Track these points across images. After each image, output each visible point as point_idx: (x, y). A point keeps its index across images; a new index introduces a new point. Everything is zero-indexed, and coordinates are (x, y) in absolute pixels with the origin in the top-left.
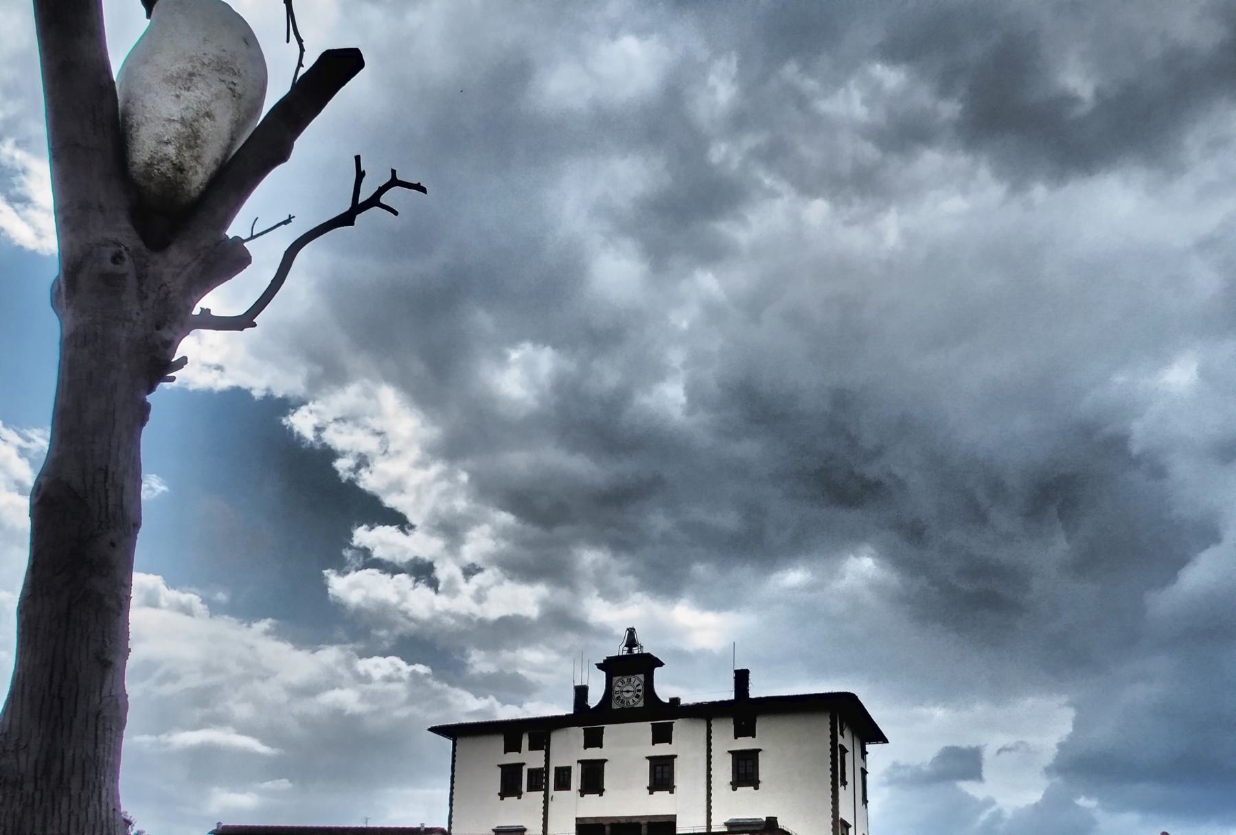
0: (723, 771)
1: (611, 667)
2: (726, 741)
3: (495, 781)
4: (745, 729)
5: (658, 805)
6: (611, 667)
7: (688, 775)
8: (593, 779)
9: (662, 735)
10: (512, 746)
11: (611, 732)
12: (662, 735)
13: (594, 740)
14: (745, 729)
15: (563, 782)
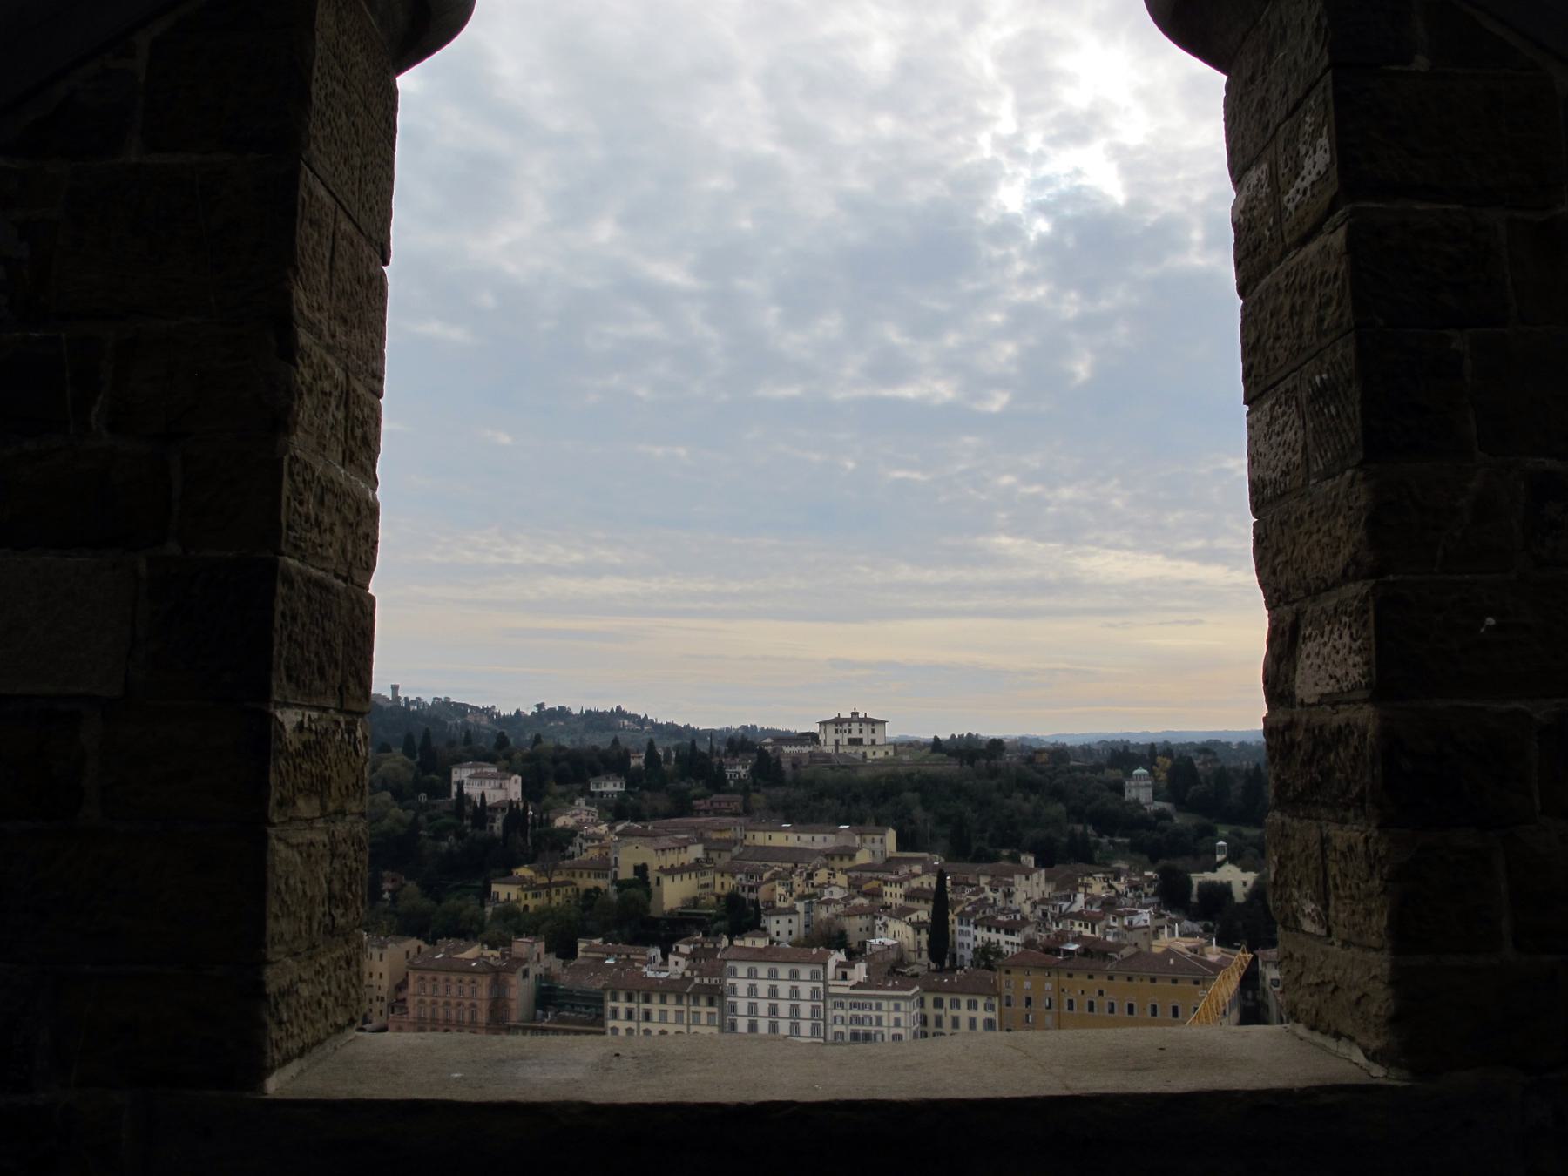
0: (870, 731)
1: (853, 714)
2: (870, 727)
3: (834, 731)
4: (873, 725)
5: (860, 736)
6: (853, 714)
7: (864, 731)
8: (850, 731)
9: (861, 725)
10: (837, 725)
11: (853, 724)
12: (861, 725)
13: (850, 725)
14: (873, 725)
15: (845, 731)
